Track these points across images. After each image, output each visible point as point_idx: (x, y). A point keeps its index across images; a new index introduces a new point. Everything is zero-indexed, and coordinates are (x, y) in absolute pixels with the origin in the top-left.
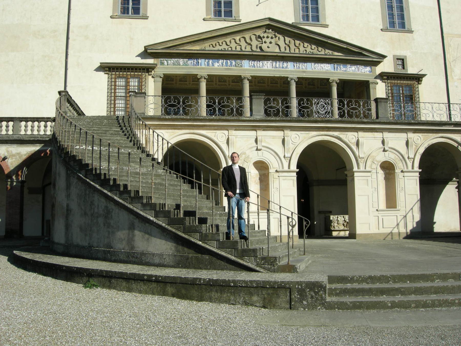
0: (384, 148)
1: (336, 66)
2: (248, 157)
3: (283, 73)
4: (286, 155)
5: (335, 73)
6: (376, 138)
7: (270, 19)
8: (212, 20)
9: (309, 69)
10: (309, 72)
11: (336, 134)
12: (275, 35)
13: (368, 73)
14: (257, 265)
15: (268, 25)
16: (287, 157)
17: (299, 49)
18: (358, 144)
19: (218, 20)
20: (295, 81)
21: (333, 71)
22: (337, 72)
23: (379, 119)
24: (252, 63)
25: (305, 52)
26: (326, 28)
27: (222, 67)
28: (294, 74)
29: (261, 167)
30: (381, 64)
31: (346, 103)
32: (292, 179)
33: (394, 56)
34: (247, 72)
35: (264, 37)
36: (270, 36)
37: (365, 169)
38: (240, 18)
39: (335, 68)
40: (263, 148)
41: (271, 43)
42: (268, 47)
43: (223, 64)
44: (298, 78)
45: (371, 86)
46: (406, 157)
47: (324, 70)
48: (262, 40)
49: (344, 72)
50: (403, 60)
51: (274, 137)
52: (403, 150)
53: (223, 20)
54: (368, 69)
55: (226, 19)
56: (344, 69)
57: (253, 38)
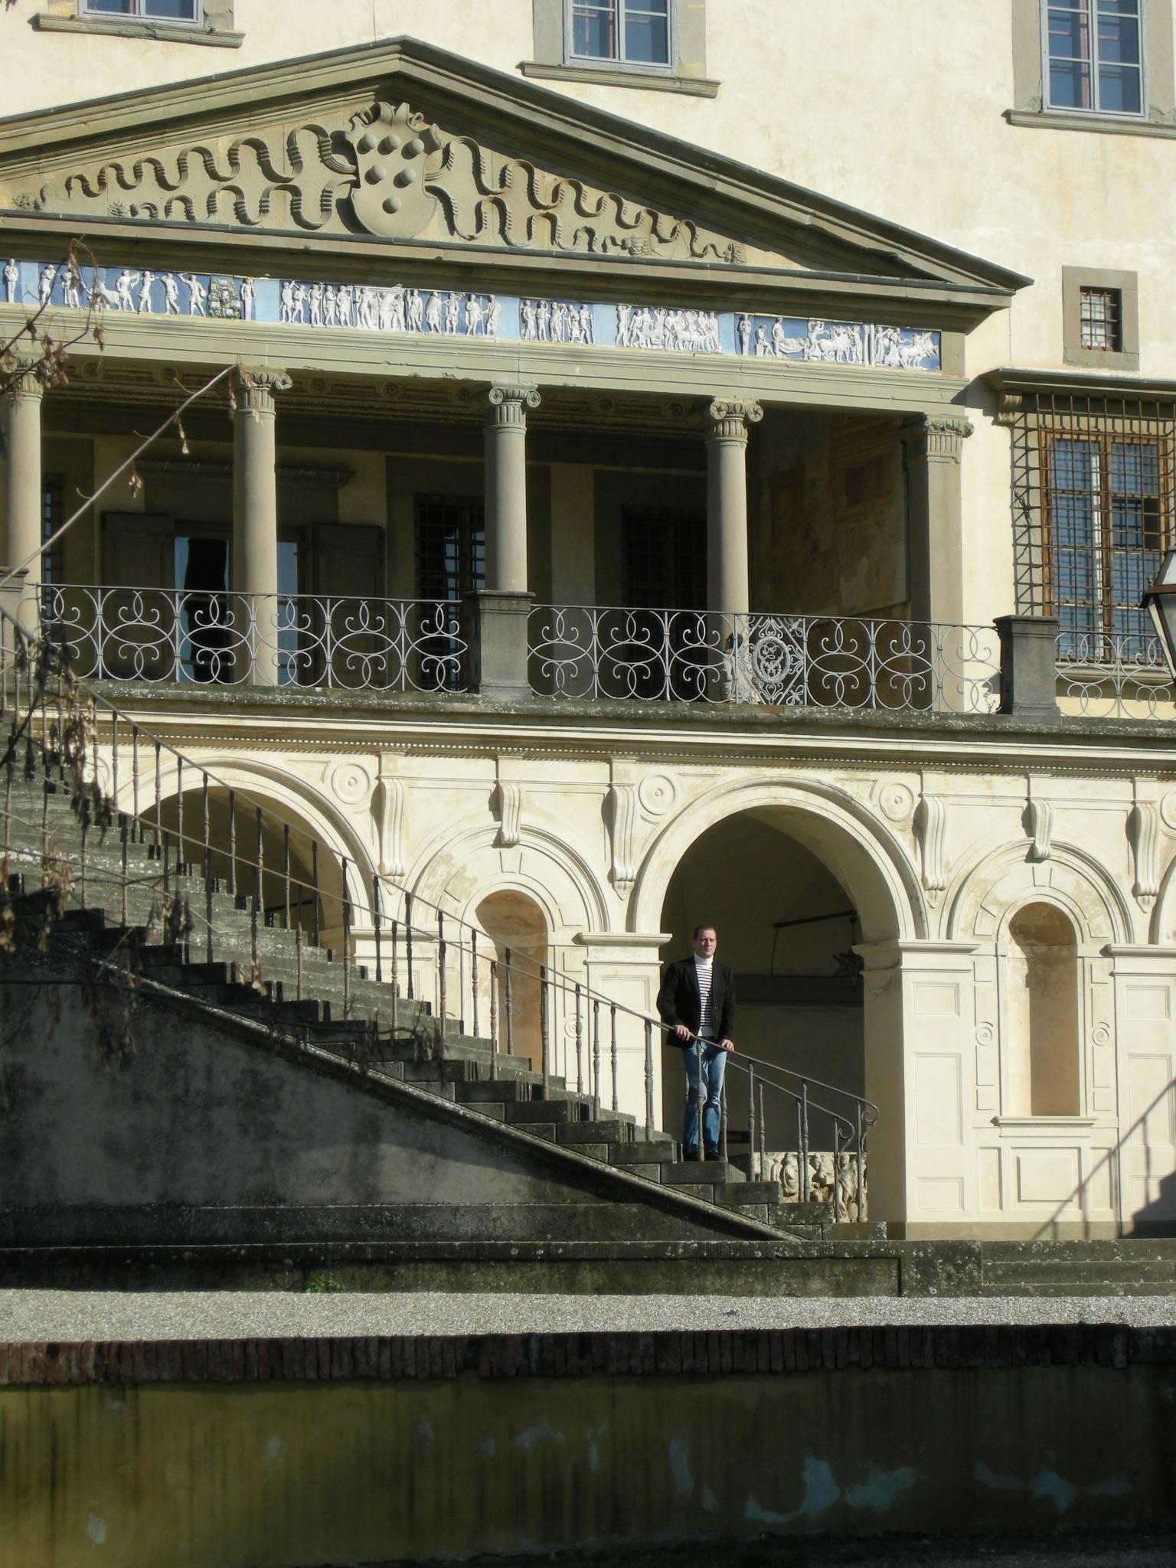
0: (1033, 848)
1: (748, 326)
2: (460, 875)
3: (463, 362)
4: (620, 871)
5: (741, 367)
6: (997, 802)
7: (410, 48)
8: (84, 28)
9: (603, 343)
10: (607, 358)
11: (829, 777)
12: (425, 136)
13: (921, 370)
14: (779, 1225)
15: (397, 76)
16: (620, 880)
17: (553, 220)
18: (919, 825)
19: (115, 29)
20: (524, 406)
21: (731, 354)
22: (751, 359)
23: (1015, 713)
24: (296, 295)
25: (582, 248)
26: (707, 101)
27: (132, 315)
28: (523, 366)
29: (508, 918)
30: (995, 316)
31: (873, 637)
32: (638, 977)
33: (1068, 273)
34: (267, 349)
35: (364, 147)
36: (399, 140)
37: (949, 936)
38: (238, 27)
39: (746, 339)
40: (525, 838)
41: (401, 181)
42: (388, 208)
43: (137, 297)
44: (543, 390)
45: (935, 445)
46: (1125, 888)
47: (684, 352)
48: (354, 161)
49: (791, 363)
50: (1115, 295)
51: (568, 788)
52: (1113, 853)
53: (145, 31)
54: (922, 344)
55: (161, 28)
56: (794, 345)
57: (308, 145)
